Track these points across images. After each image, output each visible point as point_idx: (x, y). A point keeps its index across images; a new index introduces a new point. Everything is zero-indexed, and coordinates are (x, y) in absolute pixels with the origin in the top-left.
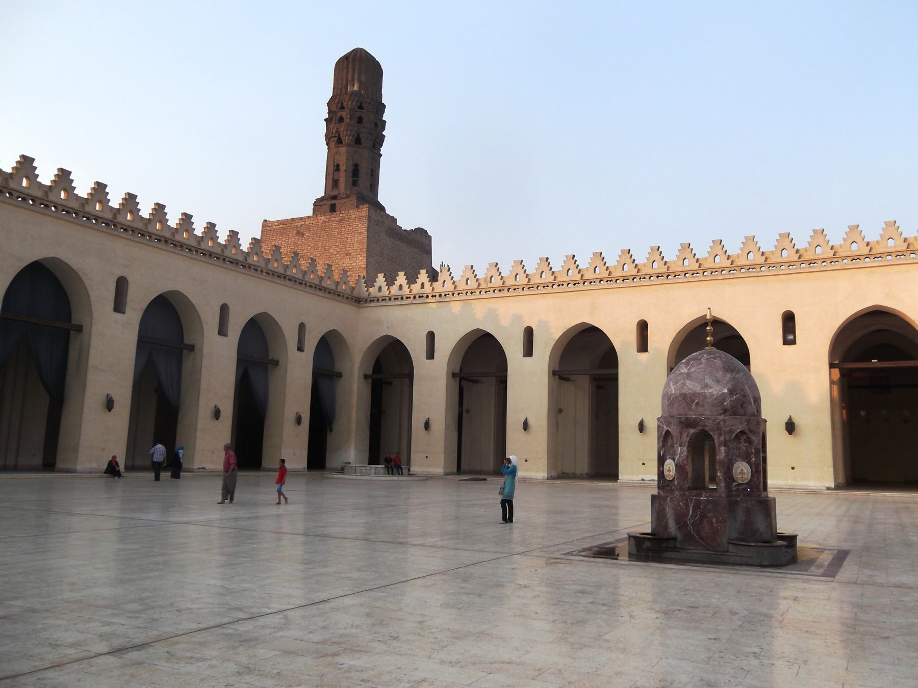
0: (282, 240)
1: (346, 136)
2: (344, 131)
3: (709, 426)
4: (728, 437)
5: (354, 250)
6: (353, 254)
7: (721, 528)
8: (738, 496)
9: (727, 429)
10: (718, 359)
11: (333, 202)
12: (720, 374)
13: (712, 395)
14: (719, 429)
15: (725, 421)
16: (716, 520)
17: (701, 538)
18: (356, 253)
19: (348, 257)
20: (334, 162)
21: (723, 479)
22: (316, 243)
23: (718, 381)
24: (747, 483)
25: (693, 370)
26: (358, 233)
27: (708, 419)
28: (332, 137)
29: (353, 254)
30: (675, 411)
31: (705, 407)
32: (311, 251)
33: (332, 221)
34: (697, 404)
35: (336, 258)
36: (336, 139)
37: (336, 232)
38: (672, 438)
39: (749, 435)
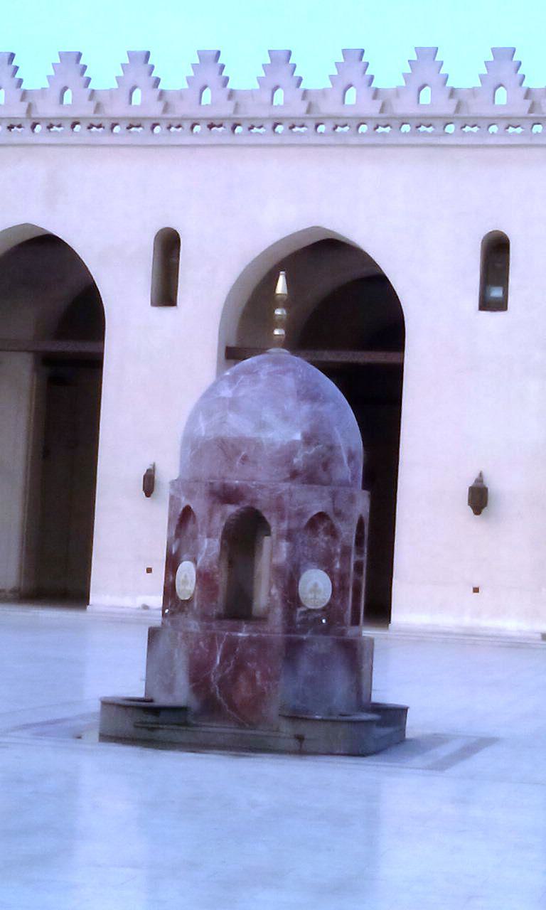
3: (263, 502)
4: (294, 524)
7: (269, 687)
8: (305, 632)
9: (296, 509)
10: (291, 374)
12: (290, 404)
13: (273, 444)
14: (279, 508)
15: (291, 494)
16: (262, 674)
17: (232, 706)
21: (280, 600)
23: (286, 418)
24: (324, 609)
25: (241, 393)
27: (262, 487)
30: (203, 470)
31: (259, 465)
34: (245, 459)
38: (194, 522)
39: (334, 521)
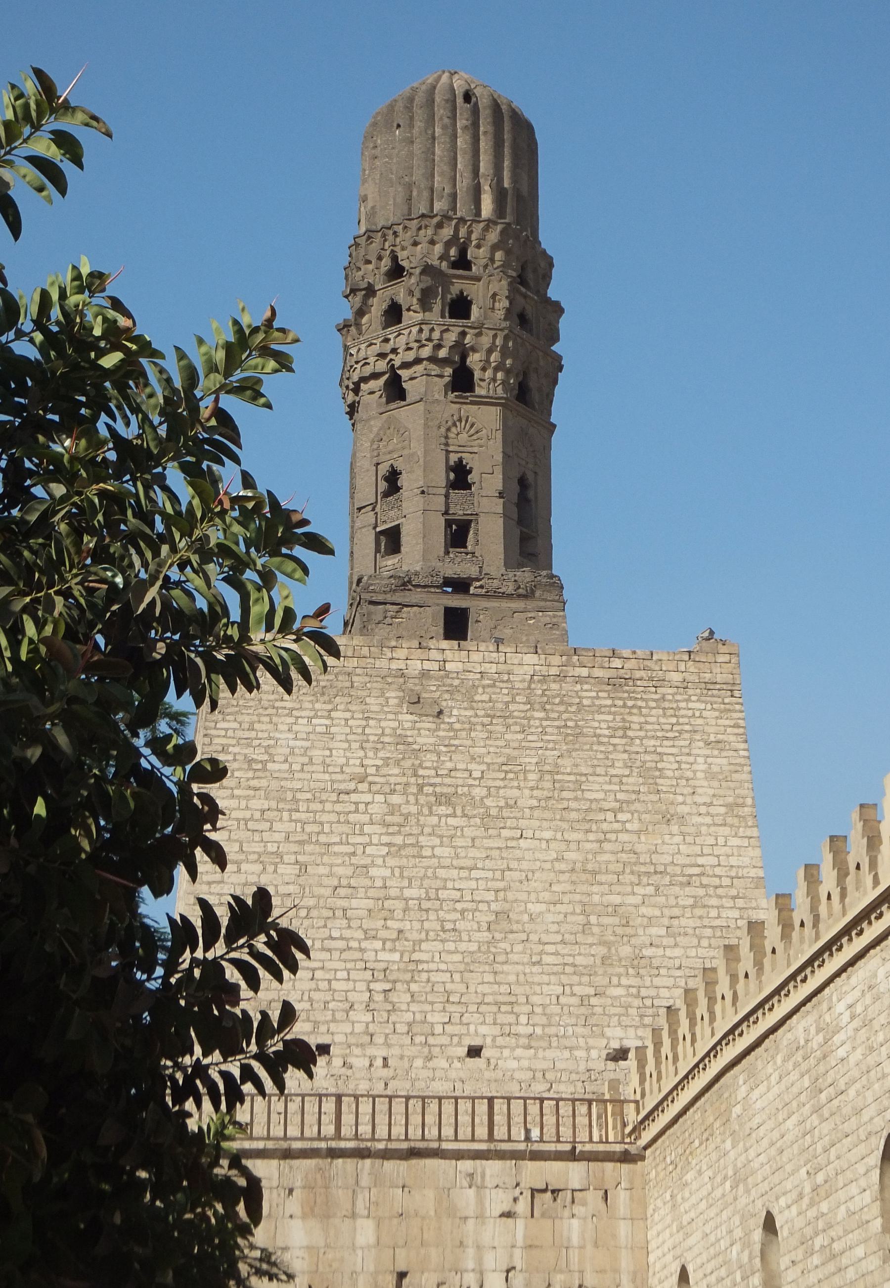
0: (329, 717)
1: (496, 369)
2: (490, 351)
5: (695, 803)
6: (697, 819)
11: (457, 601)
18: (708, 820)
19: (675, 829)
20: (448, 452)
22: (507, 751)
26: (708, 744)
28: (433, 359)
29: (697, 819)
32: (490, 783)
33: (579, 680)
35: (617, 826)
36: (449, 371)
37: (602, 723)
